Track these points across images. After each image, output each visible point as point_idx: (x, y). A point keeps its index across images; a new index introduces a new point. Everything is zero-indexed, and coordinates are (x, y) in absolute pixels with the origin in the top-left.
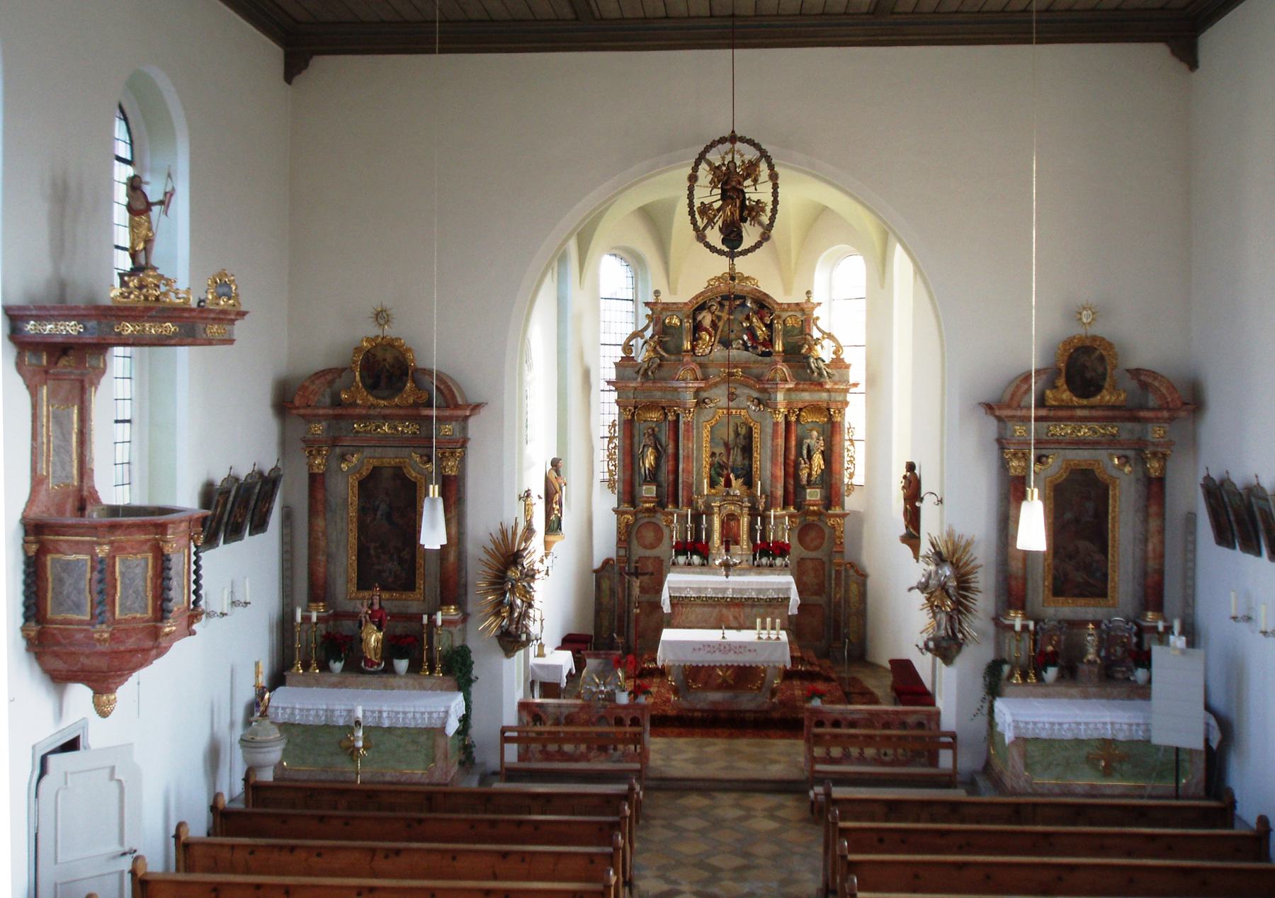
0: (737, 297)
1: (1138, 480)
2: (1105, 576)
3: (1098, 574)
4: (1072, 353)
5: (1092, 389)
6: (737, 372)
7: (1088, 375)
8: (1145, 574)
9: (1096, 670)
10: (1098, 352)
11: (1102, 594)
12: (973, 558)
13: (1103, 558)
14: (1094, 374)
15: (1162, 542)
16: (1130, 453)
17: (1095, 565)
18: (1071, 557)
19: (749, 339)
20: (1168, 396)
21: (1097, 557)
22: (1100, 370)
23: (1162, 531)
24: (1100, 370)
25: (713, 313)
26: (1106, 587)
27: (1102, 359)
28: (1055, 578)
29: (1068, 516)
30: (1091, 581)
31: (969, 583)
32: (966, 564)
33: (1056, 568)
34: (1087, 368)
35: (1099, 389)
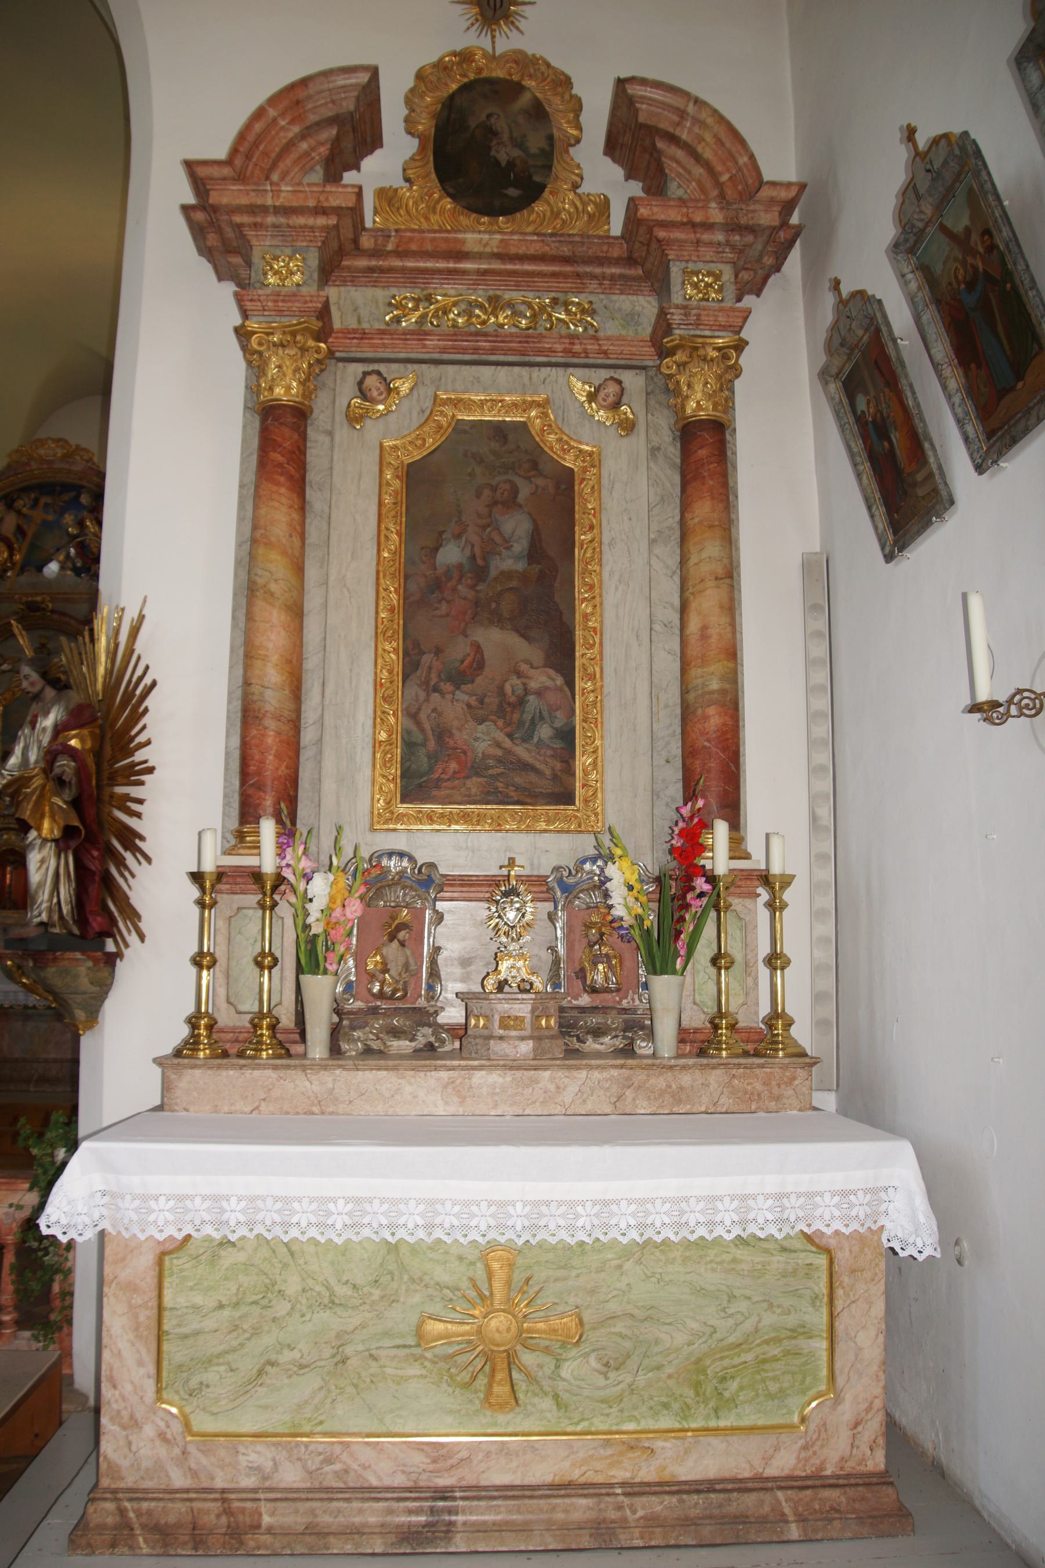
0: (66, 487)
1: (654, 452)
2: (567, 736)
3: (545, 732)
4: (452, 97)
5: (512, 192)
6: (43, 602)
7: (503, 154)
8: (687, 714)
9: (522, 1009)
10: (526, 97)
11: (567, 797)
12: (139, 672)
13: (560, 681)
14: (516, 153)
15: (731, 608)
16: (634, 381)
17: (531, 698)
18: (459, 678)
19: (78, 553)
20: (719, 168)
21: (543, 678)
22: (535, 143)
23: (730, 575)
24: (535, 143)
25: (19, 512)
26: (570, 772)
27: (538, 113)
28: (410, 746)
29: (451, 554)
30: (521, 751)
31: (131, 753)
32: (129, 695)
33: (413, 715)
34: (495, 134)
35: (533, 192)
